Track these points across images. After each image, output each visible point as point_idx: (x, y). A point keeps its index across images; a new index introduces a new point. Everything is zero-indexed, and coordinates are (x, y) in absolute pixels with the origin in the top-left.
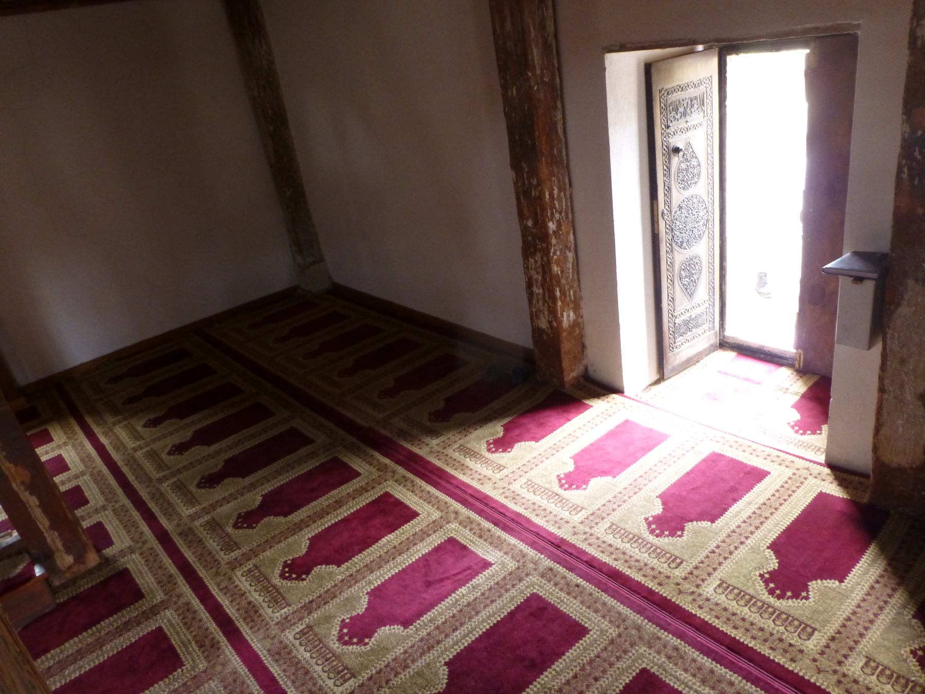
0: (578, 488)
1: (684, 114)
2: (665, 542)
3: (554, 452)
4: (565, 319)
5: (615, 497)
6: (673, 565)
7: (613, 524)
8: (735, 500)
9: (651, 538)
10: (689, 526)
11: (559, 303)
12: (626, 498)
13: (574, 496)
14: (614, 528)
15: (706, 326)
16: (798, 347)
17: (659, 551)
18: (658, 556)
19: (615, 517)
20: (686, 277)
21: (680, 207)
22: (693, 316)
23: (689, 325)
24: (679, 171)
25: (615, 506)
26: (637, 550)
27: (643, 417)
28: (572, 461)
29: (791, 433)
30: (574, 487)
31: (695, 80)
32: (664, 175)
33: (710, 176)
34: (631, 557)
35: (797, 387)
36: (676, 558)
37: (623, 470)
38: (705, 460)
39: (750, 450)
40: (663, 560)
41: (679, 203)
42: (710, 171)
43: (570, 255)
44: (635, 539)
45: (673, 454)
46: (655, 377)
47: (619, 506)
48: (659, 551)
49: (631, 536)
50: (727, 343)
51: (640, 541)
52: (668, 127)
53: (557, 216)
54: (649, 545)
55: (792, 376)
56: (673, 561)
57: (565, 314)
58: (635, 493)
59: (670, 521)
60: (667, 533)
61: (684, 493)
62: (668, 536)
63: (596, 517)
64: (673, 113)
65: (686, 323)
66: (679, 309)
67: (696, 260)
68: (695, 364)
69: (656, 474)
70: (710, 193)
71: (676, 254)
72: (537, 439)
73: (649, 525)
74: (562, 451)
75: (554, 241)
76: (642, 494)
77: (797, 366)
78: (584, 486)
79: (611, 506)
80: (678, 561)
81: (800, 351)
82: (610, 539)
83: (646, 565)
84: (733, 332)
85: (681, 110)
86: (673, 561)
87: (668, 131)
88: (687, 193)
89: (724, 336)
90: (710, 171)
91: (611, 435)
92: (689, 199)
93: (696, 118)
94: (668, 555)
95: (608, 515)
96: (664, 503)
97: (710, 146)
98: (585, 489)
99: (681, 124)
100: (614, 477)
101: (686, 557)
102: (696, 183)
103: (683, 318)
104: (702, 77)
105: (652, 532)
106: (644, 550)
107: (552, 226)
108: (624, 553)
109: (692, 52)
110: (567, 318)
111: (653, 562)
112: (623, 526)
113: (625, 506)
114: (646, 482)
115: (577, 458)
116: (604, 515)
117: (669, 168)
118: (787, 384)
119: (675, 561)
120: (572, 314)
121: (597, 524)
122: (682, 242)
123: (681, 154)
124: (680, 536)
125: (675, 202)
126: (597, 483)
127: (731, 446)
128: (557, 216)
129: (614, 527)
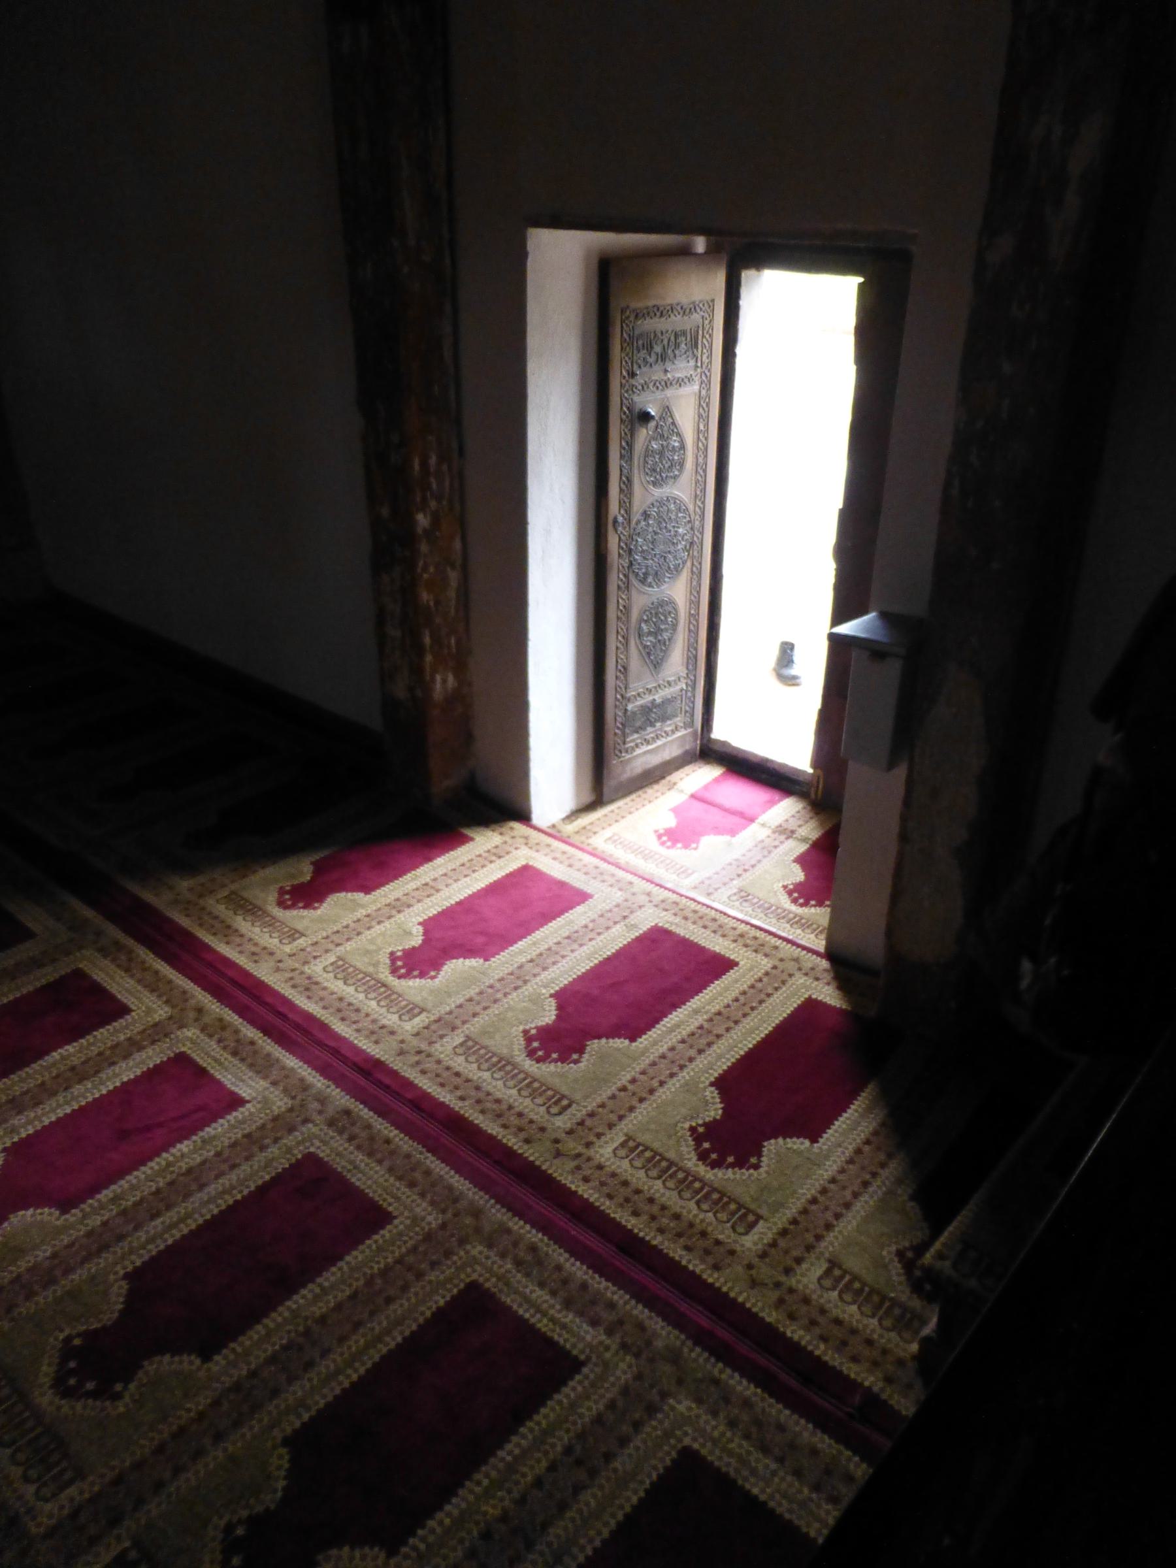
0: (422, 975)
2: (548, 1071)
3: (394, 912)
5: (481, 993)
6: (554, 1110)
7: (468, 1038)
8: (675, 1006)
9: (529, 1065)
10: (594, 1046)
12: (499, 995)
13: (414, 987)
14: (469, 1047)
17: (536, 1085)
18: (533, 1095)
19: (474, 1027)
20: (650, 633)
21: (646, 515)
22: (658, 701)
23: (653, 715)
24: (648, 453)
25: (478, 1009)
26: (500, 1083)
27: (551, 863)
28: (421, 929)
29: (785, 902)
30: (416, 973)
32: (622, 457)
33: (700, 468)
34: (488, 1094)
35: (811, 831)
36: (563, 1097)
37: (503, 949)
38: (639, 940)
39: (714, 926)
40: (539, 1101)
41: (644, 507)
42: (701, 460)
44: (502, 1064)
45: (591, 925)
47: (485, 1008)
48: (536, 1085)
49: (495, 1059)
51: (509, 1068)
54: (522, 1076)
55: (803, 812)
56: (556, 1103)
58: (516, 988)
59: (561, 1039)
60: (555, 1056)
61: (596, 992)
62: (556, 1061)
63: (445, 1024)
65: (647, 710)
66: (635, 687)
69: (558, 958)
70: (699, 497)
71: (634, 592)
72: (367, 890)
73: (529, 1039)
74: (407, 911)
76: (527, 990)
77: (813, 796)
78: (433, 973)
79: (471, 1008)
80: (565, 1102)
81: (819, 772)
82: (459, 1064)
83: (510, 1108)
84: (720, 732)
86: (556, 1103)
88: (658, 492)
90: (701, 460)
91: (495, 889)
94: (550, 1093)
95: (464, 1022)
96: (560, 1007)
97: (702, 417)
98: (433, 978)
100: (486, 960)
101: (577, 1096)
102: (675, 477)
103: (640, 702)
105: (531, 1053)
106: (511, 1083)
108: (478, 1088)
111: (525, 1104)
112: (486, 1041)
113: (495, 1009)
114: (536, 970)
115: (429, 925)
116: (458, 1022)
118: (793, 824)
119: (560, 1102)
121: (442, 1037)
122: (646, 574)
124: (576, 1062)
126: (455, 968)
127: (686, 918)
129: (470, 1043)
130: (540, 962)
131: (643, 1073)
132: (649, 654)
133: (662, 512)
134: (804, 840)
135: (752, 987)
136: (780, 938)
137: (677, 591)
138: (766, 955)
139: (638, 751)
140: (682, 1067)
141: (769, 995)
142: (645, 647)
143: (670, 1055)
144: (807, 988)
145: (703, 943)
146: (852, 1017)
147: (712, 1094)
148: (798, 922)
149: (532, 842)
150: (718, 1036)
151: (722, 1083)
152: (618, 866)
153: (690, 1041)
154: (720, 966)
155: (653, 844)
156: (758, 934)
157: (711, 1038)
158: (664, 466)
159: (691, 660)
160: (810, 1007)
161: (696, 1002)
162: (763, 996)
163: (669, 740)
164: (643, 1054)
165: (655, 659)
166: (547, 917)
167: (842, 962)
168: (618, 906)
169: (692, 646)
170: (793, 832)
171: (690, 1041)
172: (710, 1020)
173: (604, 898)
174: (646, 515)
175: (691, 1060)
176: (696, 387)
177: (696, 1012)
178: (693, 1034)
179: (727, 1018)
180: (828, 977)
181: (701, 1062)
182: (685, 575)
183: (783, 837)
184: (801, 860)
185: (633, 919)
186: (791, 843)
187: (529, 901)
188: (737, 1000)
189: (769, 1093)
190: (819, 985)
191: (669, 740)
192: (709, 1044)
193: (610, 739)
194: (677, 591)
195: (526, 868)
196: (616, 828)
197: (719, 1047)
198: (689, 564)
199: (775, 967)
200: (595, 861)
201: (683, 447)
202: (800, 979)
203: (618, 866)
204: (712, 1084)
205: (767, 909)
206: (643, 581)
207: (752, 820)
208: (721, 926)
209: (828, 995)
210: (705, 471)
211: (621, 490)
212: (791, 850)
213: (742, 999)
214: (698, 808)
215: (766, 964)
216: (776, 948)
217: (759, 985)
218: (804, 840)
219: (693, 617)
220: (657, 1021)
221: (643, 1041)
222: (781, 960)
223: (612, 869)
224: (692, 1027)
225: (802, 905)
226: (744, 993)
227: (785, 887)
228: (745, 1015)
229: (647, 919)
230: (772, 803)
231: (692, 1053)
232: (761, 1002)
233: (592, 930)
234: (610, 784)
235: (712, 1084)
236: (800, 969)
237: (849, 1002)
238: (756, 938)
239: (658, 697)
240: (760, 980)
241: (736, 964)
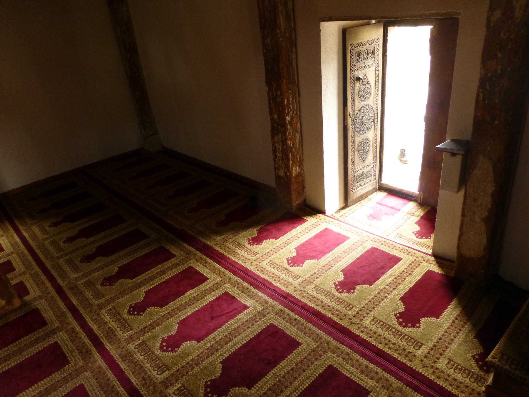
1: (363, 59)
4: (294, 171)
8: (383, 274)
10: (358, 287)
11: (291, 162)
21: (359, 111)
23: (363, 177)
24: (360, 90)
27: (335, 227)
31: (370, 40)
32: (351, 93)
33: (376, 94)
38: (367, 252)
39: (392, 246)
41: (359, 108)
43: (298, 135)
45: (351, 248)
46: (343, 205)
52: (354, 65)
53: (291, 113)
57: (294, 168)
61: (356, 269)
66: (357, 167)
67: (367, 141)
69: (341, 259)
70: (376, 104)
71: (356, 137)
75: (289, 127)
85: (362, 56)
87: (354, 68)
88: (363, 103)
91: (317, 236)
93: (370, 61)
97: (377, 77)
99: (362, 65)
102: (368, 98)
103: (359, 173)
104: (374, 38)
107: (288, 118)
109: (369, 24)
110: (296, 170)
114: (336, 263)
117: (354, 89)
120: (298, 169)
122: (360, 131)
123: (361, 81)
127: (382, 244)
128: (291, 113)
130: (336, 260)
132: (361, 157)
135: (409, 267)
138: (412, 256)
139: (358, 189)
141: (414, 269)
143: (384, 290)
144: (428, 267)
145: (389, 252)
146: (445, 276)
149: (327, 220)
154: (396, 260)
156: (408, 248)
158: (364, 95)
160: (429, 273)
161: (390, 272)
162: (413, 270)
164: (375, 290)
166: (336, 245)
167: (439, 258)
169: (375, 153)
172: (396, 278)
173: (353, 238)
176: (374, 67)
177: (391, 275)
179: (401, 278)
180: (434, 263)
182: (372, 129)
185: (364, 245)
187: (327, 242)
188: (404, 271)
190: (432, 265)
191: (369, 185)
192: (397, 286)
194: (370, 135)
195: (326, 229)
198: (373, 126)
199: (415, 260)
201: (371, 88)
202: (424, 264)
205: (408, 240)
209: (435, 269)
211: (351, 104)
213: (406, 271)
215: (412, 259)
216: (415, 253)
217: (411, 266)
219: (375, 143)
220: (378, 279)
221: (374, 285)
222: (417, 257)
224: (390, 280)
226: (406, 269)
228: (407, 276)
229: (368, 246)
232: (412, 272)
234: (350, 200)
238: (407, 250)
239: (365, 171)
240: (411, 264)
241: (402, 259)
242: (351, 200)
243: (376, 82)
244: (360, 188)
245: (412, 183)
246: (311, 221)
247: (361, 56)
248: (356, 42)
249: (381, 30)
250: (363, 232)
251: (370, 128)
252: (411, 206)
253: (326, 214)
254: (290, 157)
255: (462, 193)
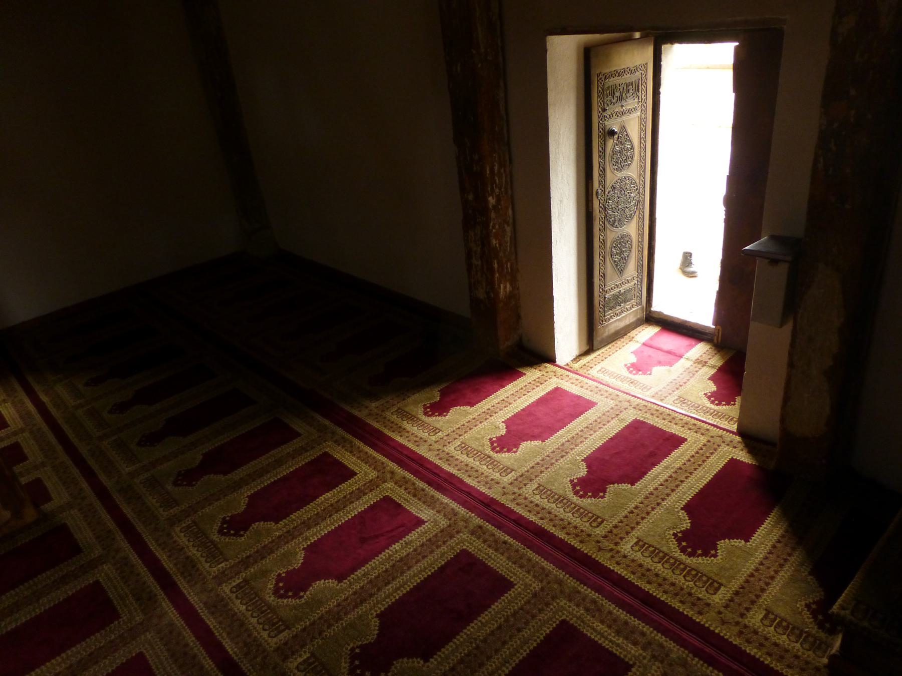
1: (620, 99)
8: (654, 465)
11: (497, 275)
15: (633, 302)
16: (716, 322)
20: (617, 254)
21: (613, 188)
23: (619, 300)
24: (614, 152)
29: (707, 403)
31: (631, 66)
32: (600, 156)
33: (642, 159)
35: (716, 361)
38: (627, 427)
43: (508, 229)
46: (585, 348)
50: (654, 318)
52: (605, 110)
57: (502, 286)
61: (607, 458)
64: (610, 97)
65: (616, 297)
66: (610, 284)
67: (627, 239)
68: (622, 337)
69: (583, 439)
70: (642, 175)
71: (608, 232)
77: (715, 341)
81: (719, 327)
84: (656, 307)
85: (617, 94)
87: (605, 114)
88: (620, 175)
89: (650, 311)
92: (621, 180)
93: (631, 103)
97: (643, 130)
99: (618, 109)
102: (629, 165)
104: (638, 63)
110: (504, 289)
117: (604, 150)
118: (705, 358)
120: (508, 286)
122: (614, 221)
123: (616, 136)
125: (609, 184)
127: (652, 414)
131: (642, 503)
133: (621, 186)
134: (713, 367)
135: (697, 453)
136: (709, 424)
137: (631, 229)
138: (702, 434)
140: (663, 499)
141: (708, 457)
142: (615, 261)
144: (730, 453)
146: (760, 468)
147: (683, 514)
148: (716, 414)
149: (558, 374)
150: (682, 481)
151: (687, 508)
152: (608, 386)
153: (665, 484)
154: (676, 441)
155: (625, 373)
156: (696, 422)
157: (678, 483)
158: (622, 160)
159: (640, 267)
160: (733, 462)
161: (666, 462)
163: (629, 313)
165: (620, 269)
167: (748, 437)
168: (612, 408)
169: (640, 260)
170: (706, 362)
171: (665, 484)
172: (676, 472)
173: (603, 404)
174: (613, 188)
175: (668, 495)
176: (639, 113)
177: (666, 468)
178: (667, 480)
179: (685, 471)
180: (741, 446)
181: (674, 497)
183: (700, 366)
184: (711, 379)
185: (621, 416)
186: (705, 369)
188: (689, 460)
189: (716, 513)
190: (737, 451)
191: (629, 313)
192: (677, 486)
193: (597, 314)
194: (631, 229)
195: (557, 389)
196: (602, 364)
197: (683, 488)
198: (637, 213)
199: (709, 441)
200: (596, 384)
201: (632, 148)
203: (608, 386)
204: (682, 509)
205: (697, 408)
206: (613, 225)
207: (681, 357)
208: (674, 418)
209: (743, 456)
210: (645, 160)
212: (706, 373)
213: (692, 460)
214: (649, 351)
215: (703, 439)
216: (708, 430)
217: (701, 452)
218: (713, 367)
219: (640, 243)
220: (645, 473)
221: (639, 485)
222: (712, 437)
223: (606, 388)
224: (666, 476)
225: (717, 405)
226: (693, 456)
227: (706, 394)
228: (695, 469)
229: (630, 416)
230: (692, 346)
231: (668, 491)
232: (704, 461)
233: (599, 423)
235: (682, 509)
236: (724, 442)
237: (756, 460)
238: (695, 425)
239: (622, 289)
240: (701, 449)
241: (686, 440)
242: (599, 339)
243: (642, 139)
244: (615, 318)
245: (701, 310)
246: (531, 375)
247: (617, 94)
248: (607, 71)
249: (650, 51)
250: (619, 393)
251: (631, 217)
252: (700, 349)
253: (557, 363)
254: (496, 266)
255: (789, 327)
